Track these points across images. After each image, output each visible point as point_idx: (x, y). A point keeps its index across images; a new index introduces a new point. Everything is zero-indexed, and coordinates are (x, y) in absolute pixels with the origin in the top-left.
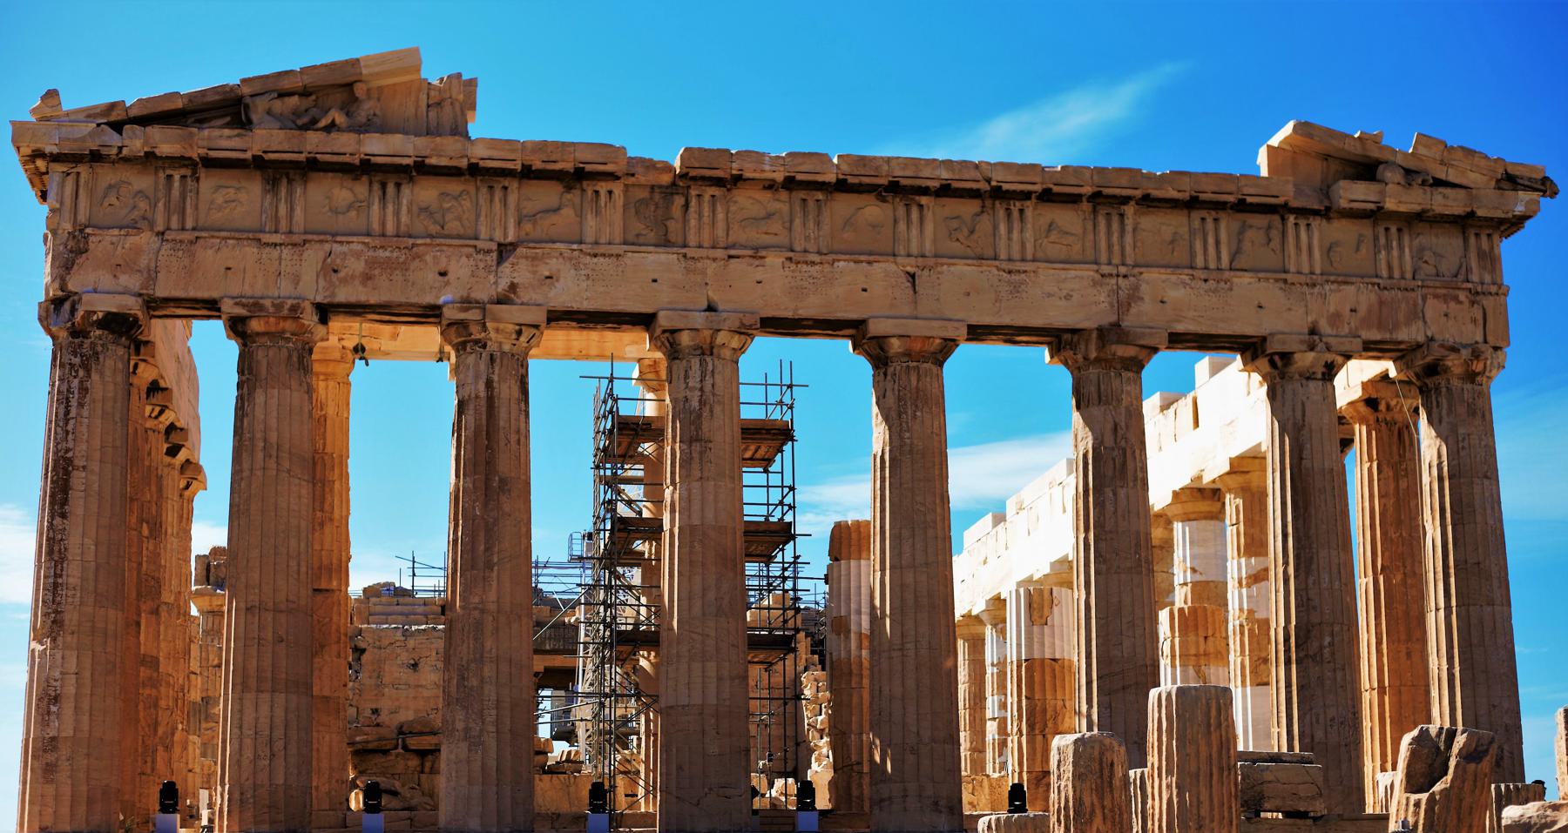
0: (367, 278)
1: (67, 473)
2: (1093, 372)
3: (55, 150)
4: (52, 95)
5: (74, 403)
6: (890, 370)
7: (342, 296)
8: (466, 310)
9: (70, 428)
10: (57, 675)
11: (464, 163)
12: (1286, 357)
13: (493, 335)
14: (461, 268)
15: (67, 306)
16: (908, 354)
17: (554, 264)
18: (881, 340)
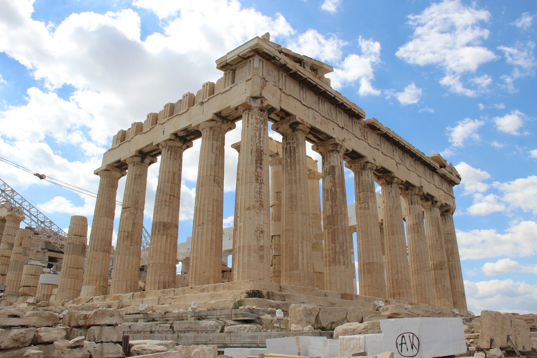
0: (321, 124)
1: (262, 155)
2: (416, 197)
3: (267, 51)
4: (268, 35)
5: (262, 132)
6: (393, 186)
7: (318, 126)
8: (339, 141)
9: (261, 139)
10: (262, 223)
11: (342, 102)
12: (436, 202)
13: (342, 150)
14: (337, 129)
15: (259, 101)
16: (397, 183)
17: (351, 136)
18: (394, 177)
